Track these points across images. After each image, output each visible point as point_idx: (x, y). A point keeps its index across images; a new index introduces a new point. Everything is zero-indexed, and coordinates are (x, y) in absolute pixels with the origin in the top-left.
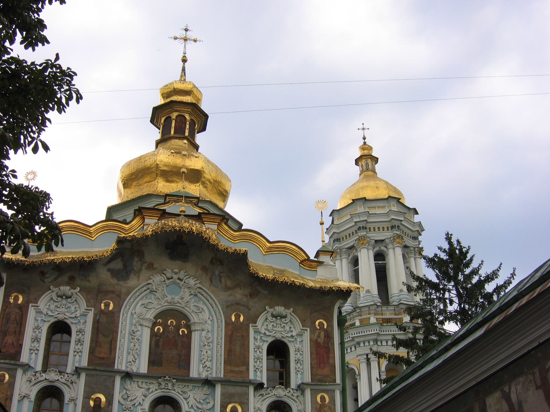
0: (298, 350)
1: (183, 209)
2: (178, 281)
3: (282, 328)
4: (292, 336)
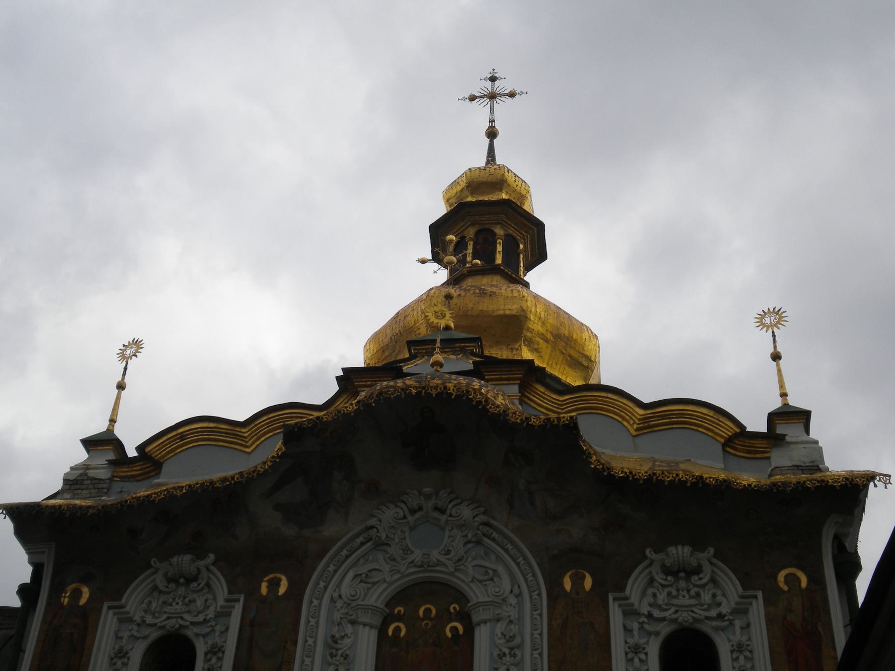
0: (739, 648)
1: (438, 357)
2: (436, 514)
3: (691, 597)
4: (720, 616)
